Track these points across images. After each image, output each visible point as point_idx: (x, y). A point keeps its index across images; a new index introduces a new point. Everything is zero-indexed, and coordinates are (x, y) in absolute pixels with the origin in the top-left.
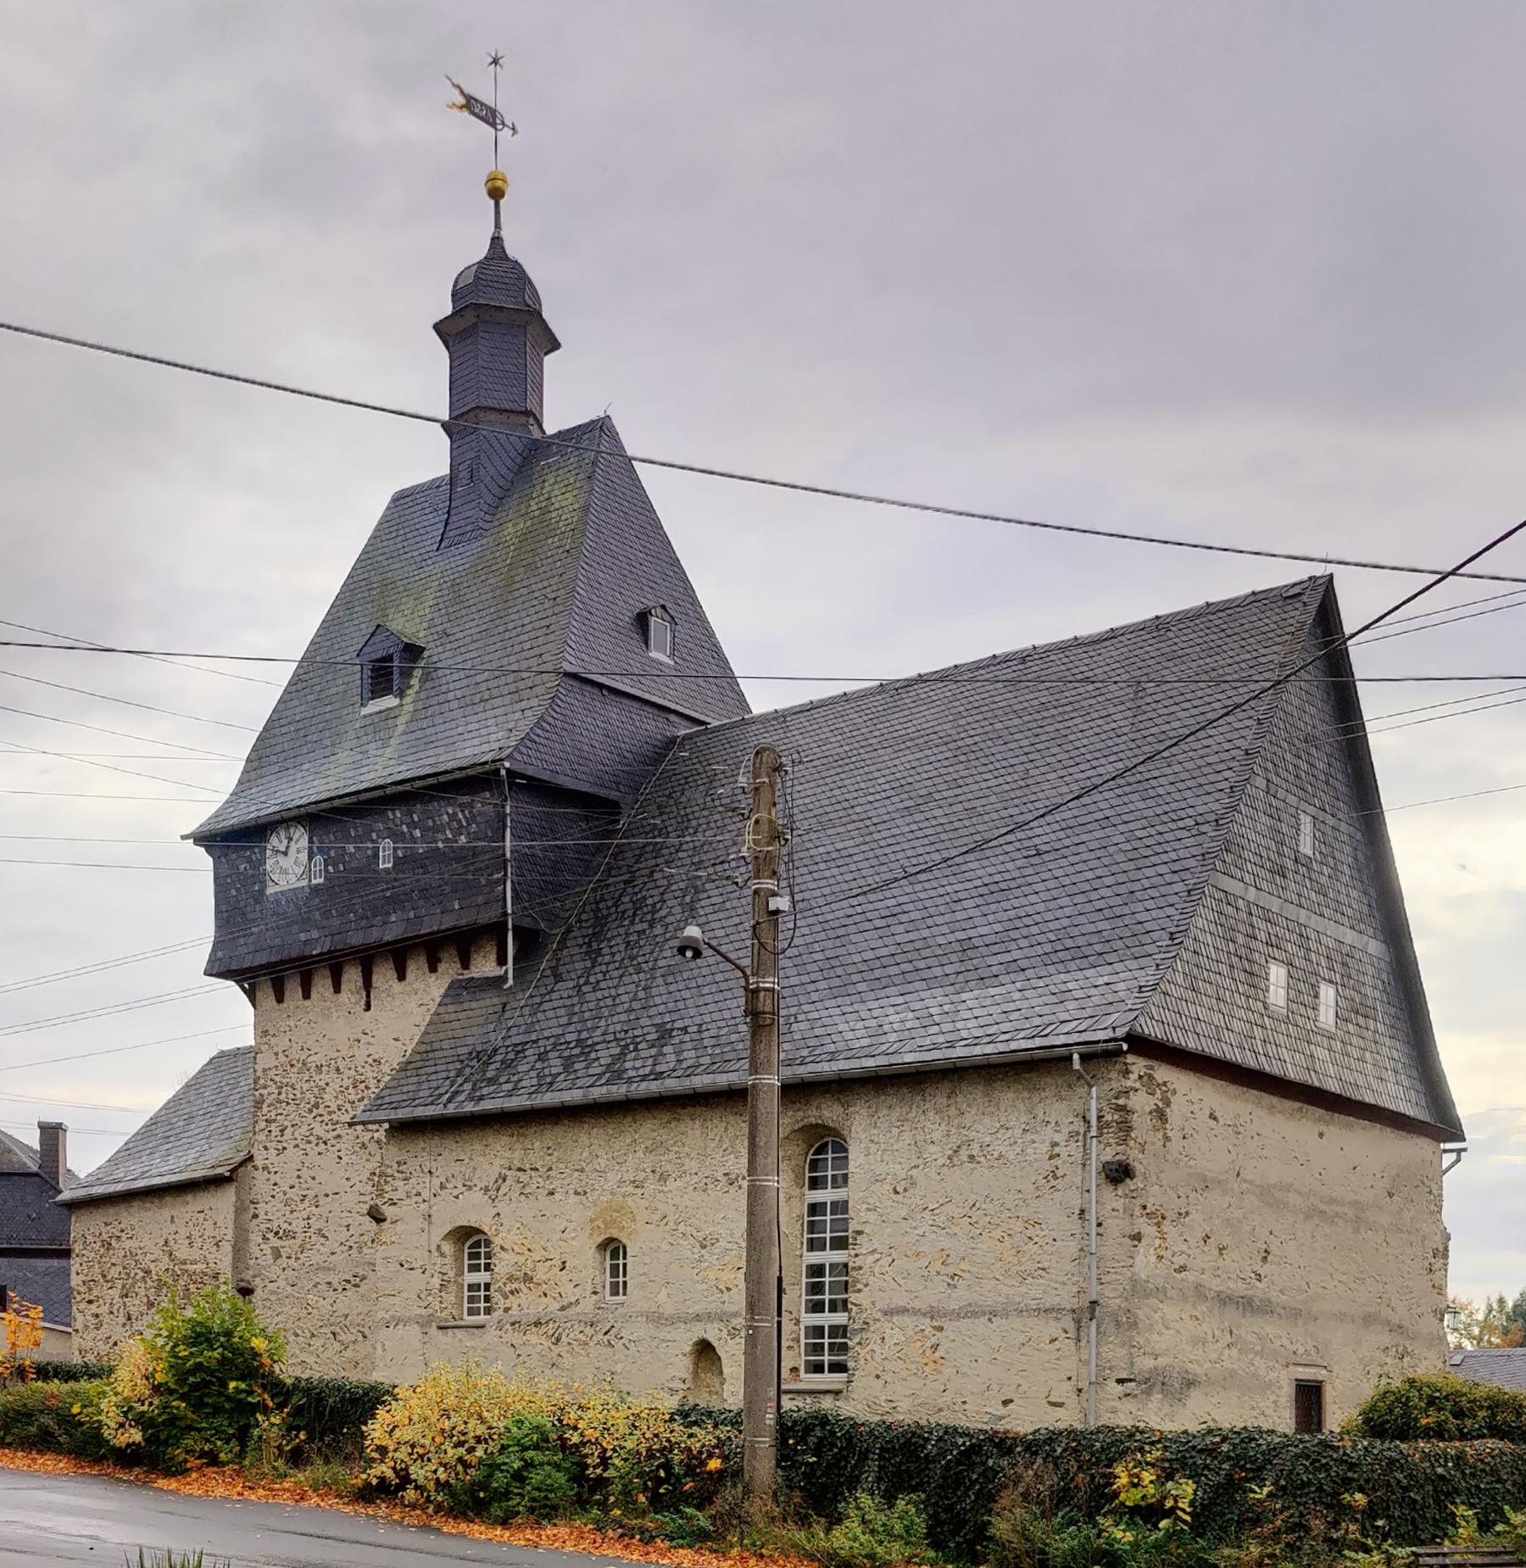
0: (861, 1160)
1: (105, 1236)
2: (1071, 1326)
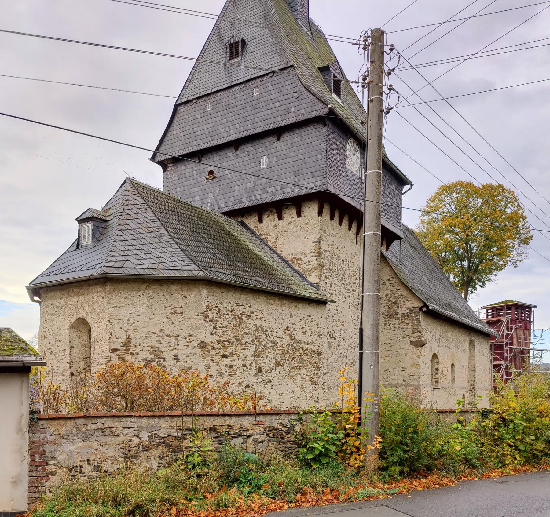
1: (237, 313)
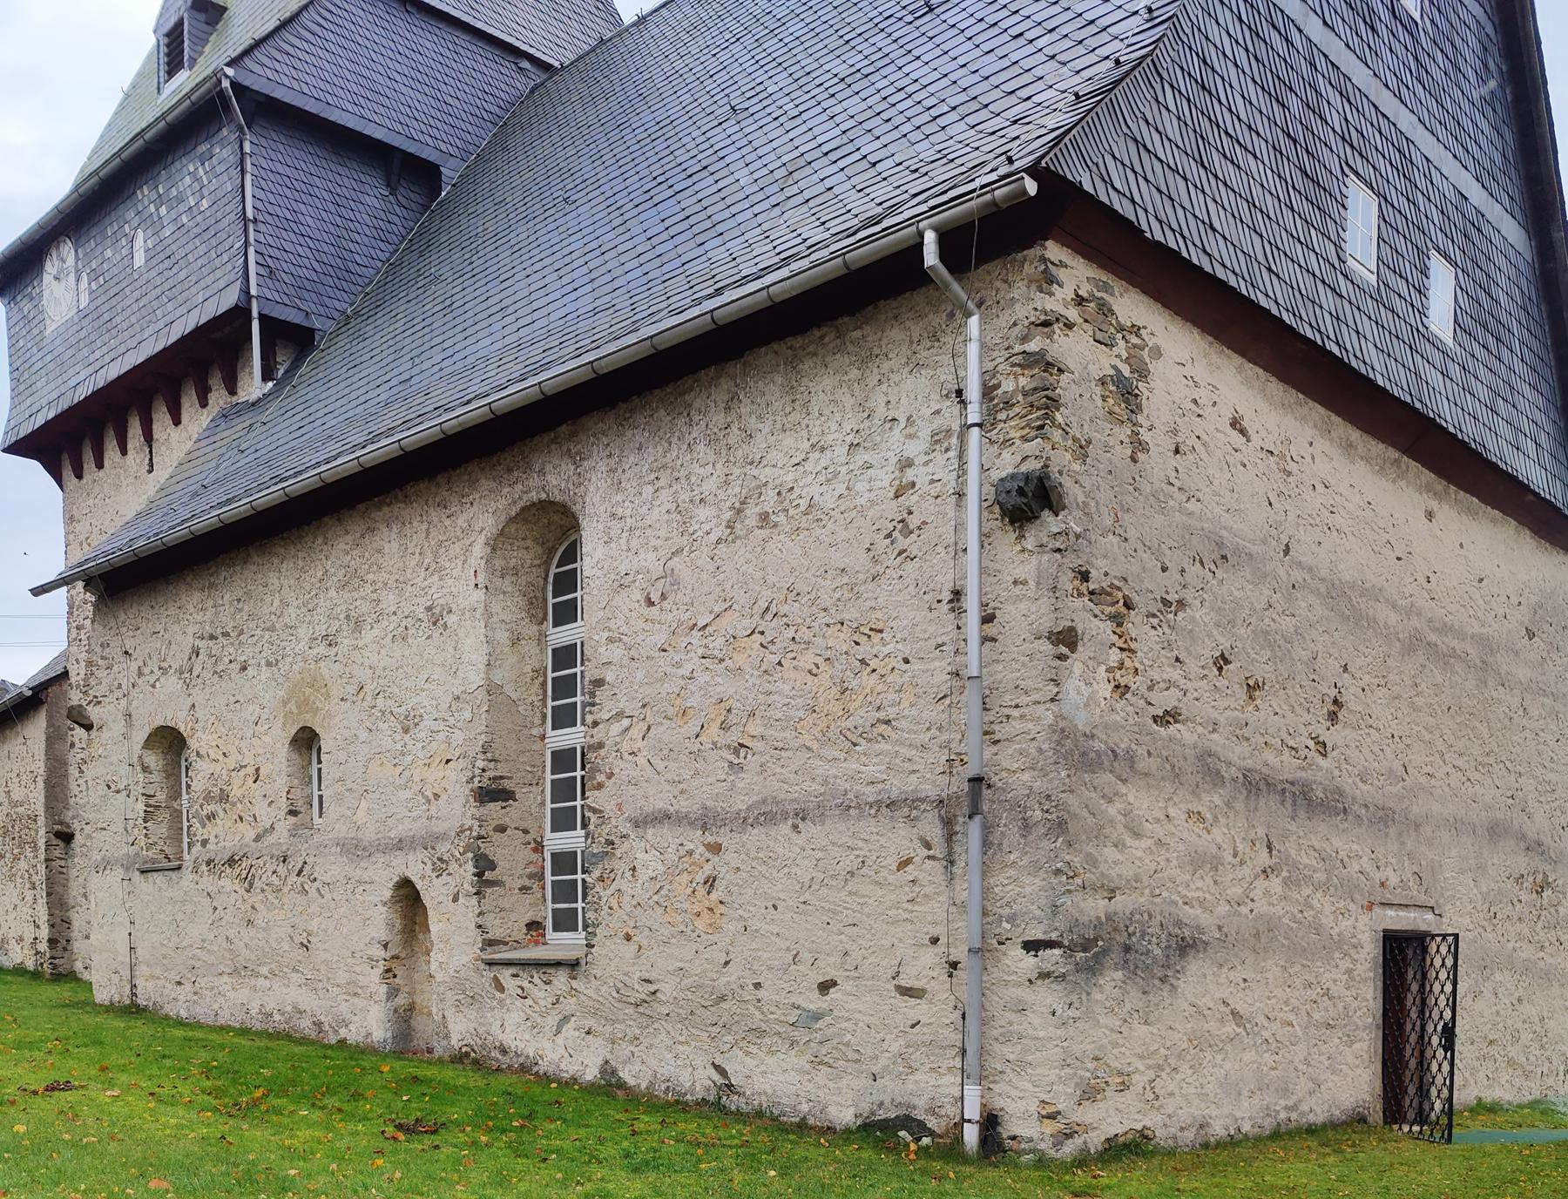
0: (599, 553)
2: (935, 832)
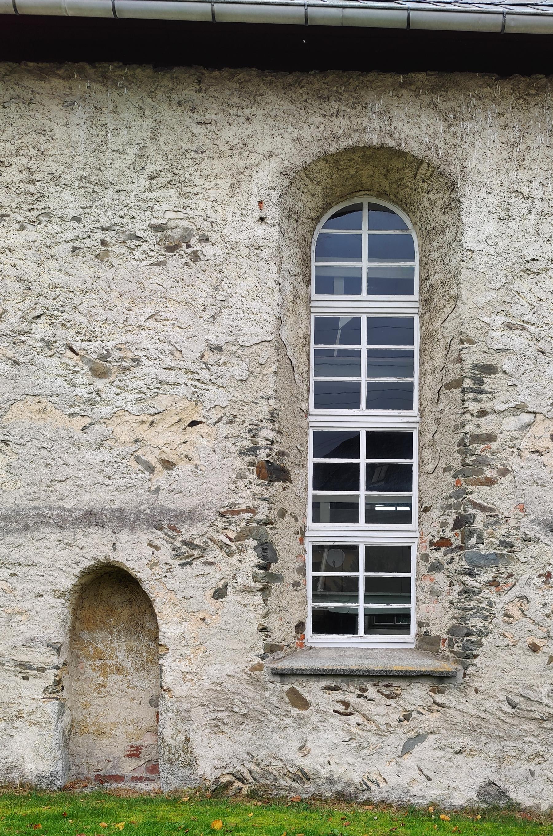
0: (491, 227)
